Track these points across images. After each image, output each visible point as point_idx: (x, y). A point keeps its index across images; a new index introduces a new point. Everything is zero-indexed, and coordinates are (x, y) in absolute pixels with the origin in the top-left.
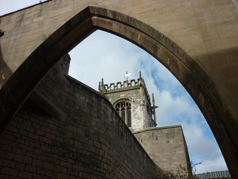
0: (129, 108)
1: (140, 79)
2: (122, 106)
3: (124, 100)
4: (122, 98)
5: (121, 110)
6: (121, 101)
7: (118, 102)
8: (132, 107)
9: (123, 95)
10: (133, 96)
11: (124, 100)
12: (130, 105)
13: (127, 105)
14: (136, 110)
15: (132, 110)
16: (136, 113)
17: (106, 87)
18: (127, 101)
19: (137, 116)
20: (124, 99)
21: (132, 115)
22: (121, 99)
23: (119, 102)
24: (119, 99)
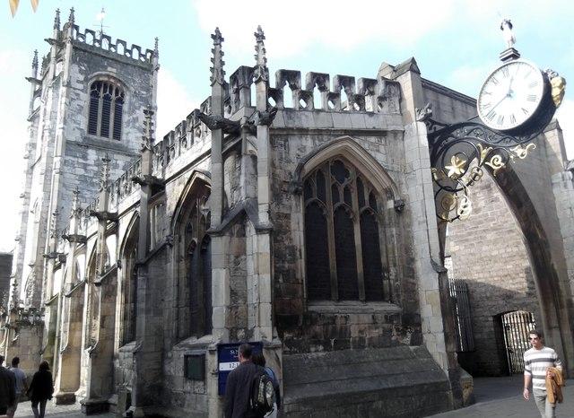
0: (120, 101)
1: (154, 54)
2: (105, 92)
3: (112, 80)
4: (111, 74)
6: (106, 79)
8: (127, 98)
9: (114, 70)
10: (134, 81)
11: (112, 80)
12: (123, 95)
13: (117, 94)
14: (137, 111)
15: (125, 107)
16: (137, 118)
19: (137, 125)
20: (114, 78)
21: (125, 118)
22: (108, 76)
23: (101, 79)
24: (104, 73)
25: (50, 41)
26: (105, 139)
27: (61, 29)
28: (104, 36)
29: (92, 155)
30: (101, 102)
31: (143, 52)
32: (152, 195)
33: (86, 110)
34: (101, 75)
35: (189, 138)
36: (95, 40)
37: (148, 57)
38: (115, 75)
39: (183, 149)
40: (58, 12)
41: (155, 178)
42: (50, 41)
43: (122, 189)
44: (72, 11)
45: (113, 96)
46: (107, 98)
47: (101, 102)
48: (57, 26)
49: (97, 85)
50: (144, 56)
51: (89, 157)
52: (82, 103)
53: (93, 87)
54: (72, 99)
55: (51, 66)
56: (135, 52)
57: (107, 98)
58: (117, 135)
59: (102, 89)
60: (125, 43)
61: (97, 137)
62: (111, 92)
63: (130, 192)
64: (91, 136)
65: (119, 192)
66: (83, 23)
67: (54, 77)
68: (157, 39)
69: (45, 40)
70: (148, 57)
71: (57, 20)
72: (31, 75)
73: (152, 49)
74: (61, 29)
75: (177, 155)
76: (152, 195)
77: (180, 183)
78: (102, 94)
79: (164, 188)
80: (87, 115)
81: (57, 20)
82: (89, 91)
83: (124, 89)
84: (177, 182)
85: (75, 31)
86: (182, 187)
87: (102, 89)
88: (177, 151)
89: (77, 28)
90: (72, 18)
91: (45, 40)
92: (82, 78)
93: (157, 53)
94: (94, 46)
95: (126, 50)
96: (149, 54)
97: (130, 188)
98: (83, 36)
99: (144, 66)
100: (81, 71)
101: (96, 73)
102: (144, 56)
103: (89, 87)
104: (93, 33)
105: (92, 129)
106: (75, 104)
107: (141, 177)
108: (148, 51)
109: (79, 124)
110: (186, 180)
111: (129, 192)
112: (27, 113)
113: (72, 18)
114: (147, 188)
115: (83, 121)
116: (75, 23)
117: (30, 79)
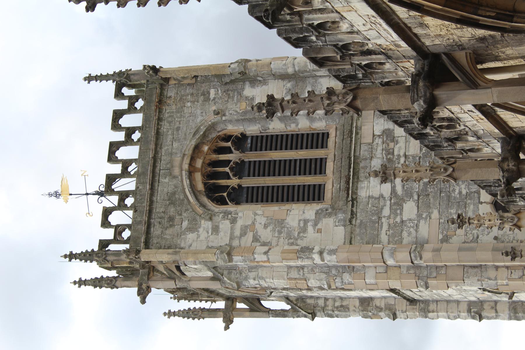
0: (240, 141)
1: (122, 80)
2: (226, 176)
3: (199, 163)
4: (186, 166)
5: (240, 178)
6: (198, 177)
7: (200, 191)
11: (199, 163)
12: (227, 138)
13: (228, 151)
17: (112, 247)
18: (206, 148)
20: (193, 159)
22: (191, 173)
23: (200, 186)
24: (186, 182)
25: (143, 294)
26: (330, 166)
27: (113, 273)
28: (108, 190)
29: (371, 188)
30: (249, 182)
31: (124, 105)
32: (456, 80)
33: (274, 210)
34: (193, 187)
35: (317, 19)
36: (121, 206)
37: (132, 92)
38: (187, 161)
39: (344, 27)
40: (81, 283)
41: (415, 78)
42: (143, 294)
43: (446, 133)
44: (71, 256)
45: (234, 156)
46: (240, 170)
47: (249, 182)
48: (111, 283)
49: (216, 194)
50: (132, 100)
51: (376, 194)
52: (261, 220)
53: (221, 202)
54: (256, 239)
55: (195, 285)
56: (126, 121)
57: (240, 170)
58: (319, 140)
59: (223, 182)
60: (112, 144)
61: (330, 181)
62: (226, 163)
63: (450, 119)
64: (328, 195)
65: (452, 140)
66: (92, 236)
67: (214, 279)
68: (89, 79)
69: (143, 301)
70: (132, 92)
71: (98, 283)
72: (219, 322)
73: (110, 86)
74: (113, 273)
75: (358, 39)
76: (456, 80)
77: (422, 25)
78: (234, 182)
79: (436, 57)
80: (287, 206)
81: (98, 283)
82: (231, 208)
83: (214, 135)
84: (418, 31)
85: (112, 247)
86: (429, 20)
87: (223, 182)
88: (348, 39)
89: (104, 244)
90: (87, 256)
91: (143, 301)
92: (206, 224)
93: (120, 74)
94: (134, 207)
95: (128, 141)
96: (126, 91)
97: (443, 119)
98: (119, 229)
99: (155, 98)
100: (193, 228)
101: (191, 199)
102: (132, 100)
103: (223, 208)
104: (107, 212)
105: (314, 194)
106: (266, 234)
107: (419, 107)
108: (119, 95)
109: (306, 222)
110: (413, 13)
111: (452, 122)
112: (303, 322)
113: (87, 256)
114: (441, 93)
115: (297, 213)
116: (96, 249)
117: (228, 322)
